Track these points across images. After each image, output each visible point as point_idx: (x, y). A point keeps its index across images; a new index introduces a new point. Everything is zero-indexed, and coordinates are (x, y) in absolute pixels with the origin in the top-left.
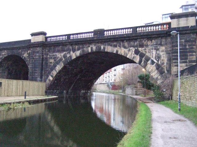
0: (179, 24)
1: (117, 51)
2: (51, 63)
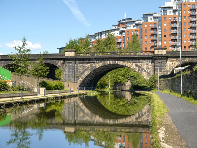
0: (158, 53)
1: (125, 64)
2: (81, 70)
